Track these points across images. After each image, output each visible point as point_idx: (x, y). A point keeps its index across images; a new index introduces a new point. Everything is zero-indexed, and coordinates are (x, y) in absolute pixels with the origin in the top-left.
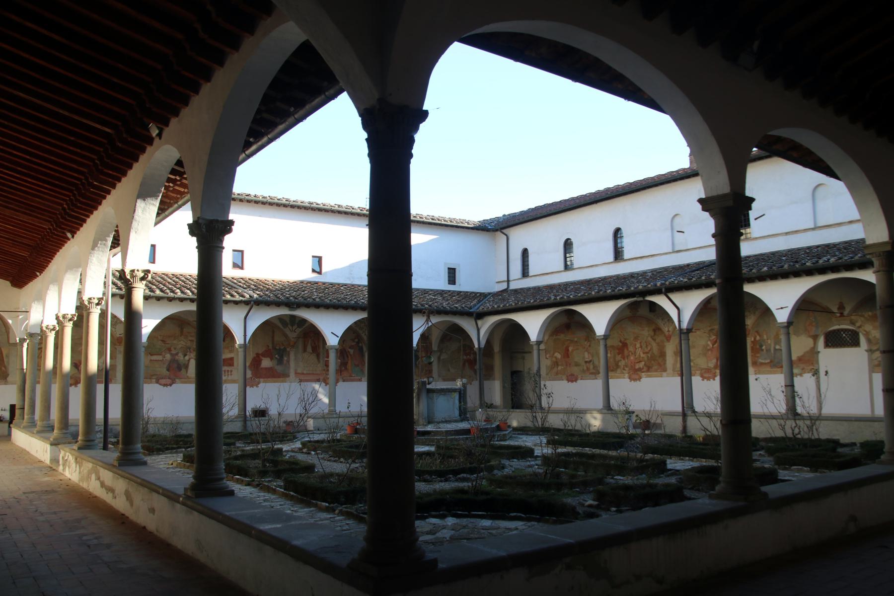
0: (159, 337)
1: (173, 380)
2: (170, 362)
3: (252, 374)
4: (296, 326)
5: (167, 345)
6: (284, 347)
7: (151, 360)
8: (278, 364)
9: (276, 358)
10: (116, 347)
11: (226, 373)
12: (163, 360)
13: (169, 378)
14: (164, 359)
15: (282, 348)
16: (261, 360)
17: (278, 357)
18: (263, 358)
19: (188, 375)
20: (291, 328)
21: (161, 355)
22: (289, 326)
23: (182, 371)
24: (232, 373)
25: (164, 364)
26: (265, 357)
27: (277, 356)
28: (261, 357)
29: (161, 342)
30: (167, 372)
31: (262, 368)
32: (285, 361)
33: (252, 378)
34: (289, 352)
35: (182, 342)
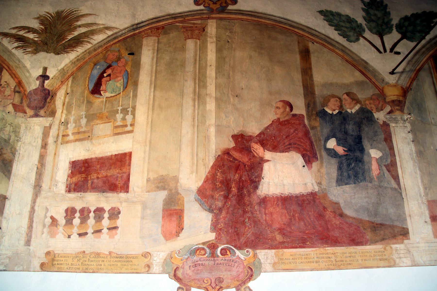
3: (215, 227)
4: (395, 35)
6: (357, 107)
8: (340, 181)
9: (332, 153)
11: (91, 221)
15: (353, 109)
16: (262, 161)
17: (340, 150)
18: (268, 155)
20: (377, 41)
22: (368, 34)
24: (119, 222)
26: (275, 148)
27: (332, 144)
28: (258, 149)
31: (264, 201)
32: (374, 166)
33: (213, 246)
34: (386, 125)
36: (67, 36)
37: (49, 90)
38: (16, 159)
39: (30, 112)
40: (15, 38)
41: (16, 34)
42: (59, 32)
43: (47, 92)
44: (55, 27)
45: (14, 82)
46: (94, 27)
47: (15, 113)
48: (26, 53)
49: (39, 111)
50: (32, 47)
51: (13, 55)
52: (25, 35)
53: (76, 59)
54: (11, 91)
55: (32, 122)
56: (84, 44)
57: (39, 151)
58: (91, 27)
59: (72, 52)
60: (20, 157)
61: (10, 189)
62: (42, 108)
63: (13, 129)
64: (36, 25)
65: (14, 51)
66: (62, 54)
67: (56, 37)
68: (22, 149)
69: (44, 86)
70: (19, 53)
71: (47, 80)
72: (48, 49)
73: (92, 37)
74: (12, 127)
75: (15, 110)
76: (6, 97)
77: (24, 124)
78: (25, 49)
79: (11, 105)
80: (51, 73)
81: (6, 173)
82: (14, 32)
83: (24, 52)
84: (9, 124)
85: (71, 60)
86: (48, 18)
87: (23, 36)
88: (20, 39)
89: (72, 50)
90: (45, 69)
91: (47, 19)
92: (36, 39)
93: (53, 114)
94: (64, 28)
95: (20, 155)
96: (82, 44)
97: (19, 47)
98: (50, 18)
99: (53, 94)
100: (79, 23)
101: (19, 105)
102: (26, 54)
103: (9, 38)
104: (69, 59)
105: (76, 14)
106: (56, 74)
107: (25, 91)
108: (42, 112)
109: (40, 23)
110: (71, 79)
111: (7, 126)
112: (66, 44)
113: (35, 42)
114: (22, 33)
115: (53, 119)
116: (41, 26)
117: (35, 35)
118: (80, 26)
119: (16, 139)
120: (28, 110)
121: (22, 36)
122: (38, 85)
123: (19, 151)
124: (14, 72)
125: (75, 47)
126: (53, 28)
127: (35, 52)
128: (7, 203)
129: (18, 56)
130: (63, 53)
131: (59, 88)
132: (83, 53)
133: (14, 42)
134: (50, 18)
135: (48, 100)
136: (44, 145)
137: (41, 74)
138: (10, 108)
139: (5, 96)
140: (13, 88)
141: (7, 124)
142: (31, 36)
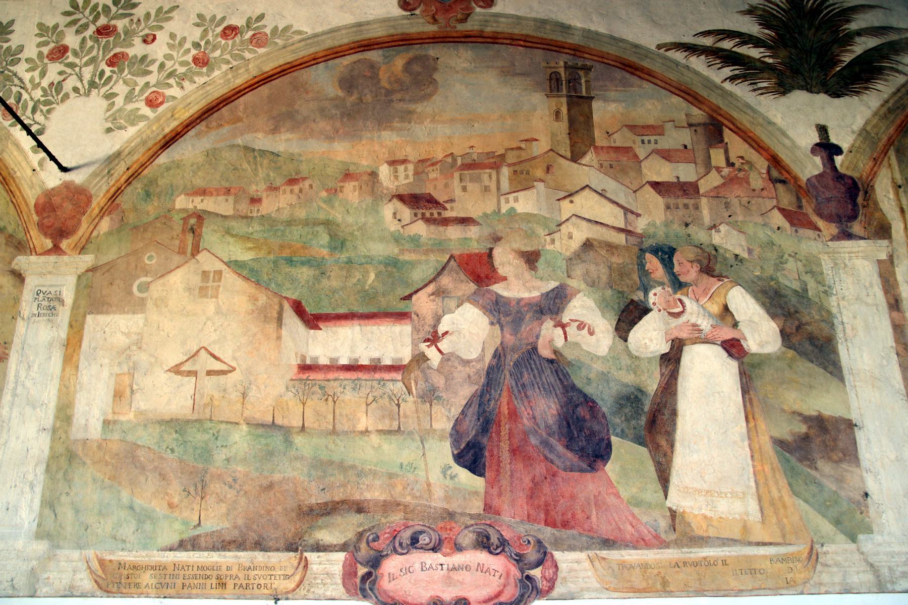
0: (384, 171)
1: (519, 559)
2: (492, 374)
5: (454, 233)
7: (305, 368)
10: (22, 262)
12: (420, 359)
13: (484, 543)
14: (432, 353)
19: (675, 499)
21: (401, 316)
23: (611, 468)
25: (430, 396)
29: (406, 213)
30: (464, 475)
35: (587, 204)
36: (838, 55)
37: (851, 178)
38: (840, 335)
39: (829, 229)
40: (717, 57)
41: (717, 48)
42: (815, 46)
43: (850, 181)
44: (800, 33)
45: (763, 159)
46: (894, 37)
47: (794, 229)
48: (760, 92)
49: (849, 224)
50: (769, 79)
51: (732, 96)
52: (735, 49)
53: (884, 109)
54: (762, 178)
55: (842, 250)
56: (888, 75)
57: (887, 316)
58: (885, 36)
59: (867, 92)
60: (847, 331)
61: (854, 404)
62: (853, 217)
63: (804, 266)
64: (751, 27)
65: (727, 85)
66: (847, 97)
67: (814, 57)
68: (844, 312)
69: (835, 167)
70: (741, 90)
71: (837, 155)
72: (807, 83)
73: (898, 58)
74: (799, 263)
75: (792, 224)
76: (757, 192)
77: (826, 255)
78: (755, 83)
79: (776, 211)
80: (842, 138)
81: (831, 368)
82: (708, 41)
83: (755, 90)
84: (790, 255)
85: (874, 109)
86: (775, 12)
87: (735, 52)
88: (729, 58)
89: (867, 88)
90: (823, 130)
91: (773, 15)
92: (770, 61)
93: (883, 231)
94: (824, 37)
95: (846, 325)
96: (882, 74)
97: (739, 78)
98: (778, 12)
99: (866, 186)
100: (853, 26)
101: (795, 212)
102: (762, 94)
103: (703, 57)
104: (869, 108)
105: (836, 6)
106: (855, 141)
107: (796, 179)
108: (856, 228)
109: (760, 24)
110: (892, 154)
111: (787, 260)
112: (845, 73)
113: (770, 68)
114: (727, 45)
115: (891, 242)
116: (766, 31)
117: (762, 50)
118: (859, 33)
119: (821, 289)
120: (821, 223)
121: (730, 51)
122: (821, 166)
123: (838, 315)
124: (751, 135)
125: (868, 81)
126: (797, 36)
127: (782, 90)
128: (860, 436)
129: (745, 99)
130: (847, 95)
131: (873, 174)
132: (894, 94)
133: (720, 66)
134: (778, 12)
135: (860, 200)
136: (892, 301)
137: (817, 140)
138: (777, 219)
139: (754, 190)
140: (764, 171)
141: (786, 256)
142: (755, 53)
